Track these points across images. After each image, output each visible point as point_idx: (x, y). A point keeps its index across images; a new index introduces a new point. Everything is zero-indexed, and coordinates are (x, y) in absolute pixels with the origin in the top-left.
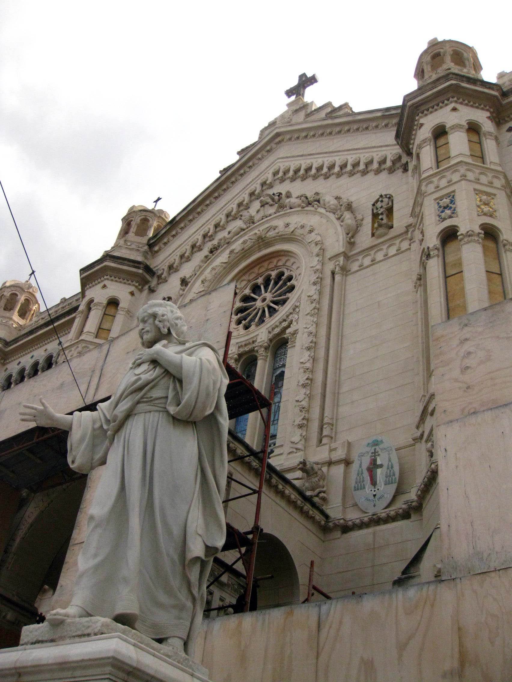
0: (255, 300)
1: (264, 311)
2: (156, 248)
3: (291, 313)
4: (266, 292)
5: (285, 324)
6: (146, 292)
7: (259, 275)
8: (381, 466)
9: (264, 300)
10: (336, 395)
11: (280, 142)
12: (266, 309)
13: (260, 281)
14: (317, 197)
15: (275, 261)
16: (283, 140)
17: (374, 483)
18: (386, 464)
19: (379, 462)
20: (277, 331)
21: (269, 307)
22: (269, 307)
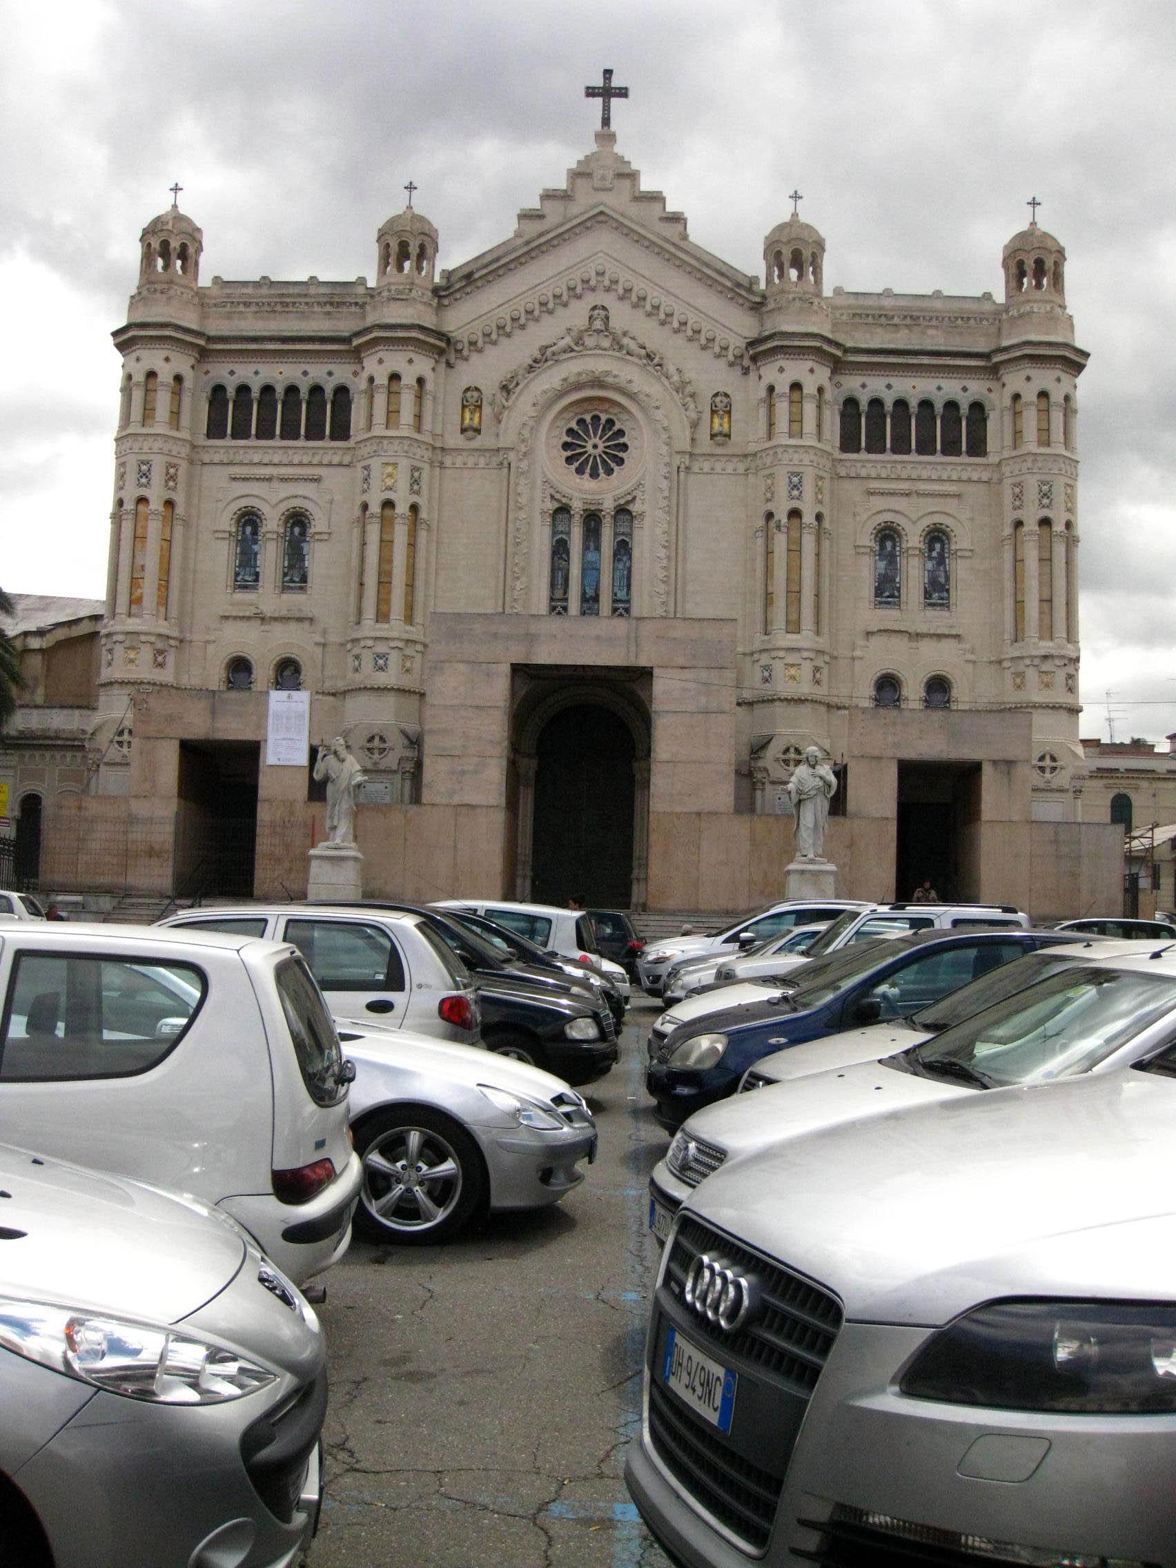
2: (446, 302)
5: (629, 498)
6: (444, 365)
7: (587, 411)
11: (602, 222)
14: (661, 362)
15: (607, 406)
16: (606, 222)
20: (622, 501)
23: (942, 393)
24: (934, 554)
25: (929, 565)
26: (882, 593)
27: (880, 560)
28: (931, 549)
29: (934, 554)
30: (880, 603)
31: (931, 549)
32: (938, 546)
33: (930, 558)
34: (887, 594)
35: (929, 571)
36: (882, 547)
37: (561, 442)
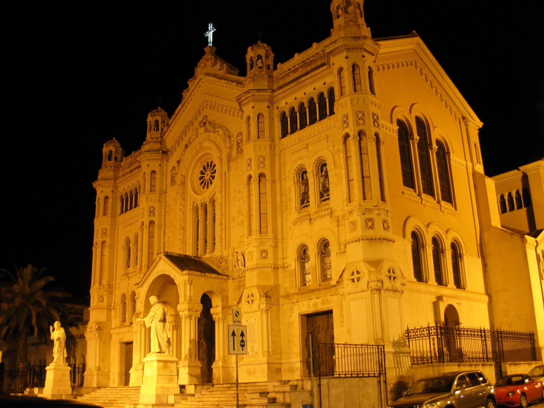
0: (204, 176)
1: (210, 178)
3: (215, 188)
4: (206, 171)
5: (214, 192)
8: (239, 260)
9: (208, 175)
10: (229, 228)
12: (210, 177)
13: (205, 164)
17: (238, 265)
18: (240, 259)
19: (239, 259)
20: (212, 195)
21: (211, 176)
22: (211, 176)
23: (316, 90)
24: (323, 173)
25: (321, 181)
26: (303, 203)
27: (302, 185)
28: (322, 171)
29: (323, 173)
30: (304, 207)
31: (322, 171)
32: (324, 168)
33: (322, 176)
34: (306, 201)
35: (322, 183)
36: (303, 178)
37: (198, 178)
